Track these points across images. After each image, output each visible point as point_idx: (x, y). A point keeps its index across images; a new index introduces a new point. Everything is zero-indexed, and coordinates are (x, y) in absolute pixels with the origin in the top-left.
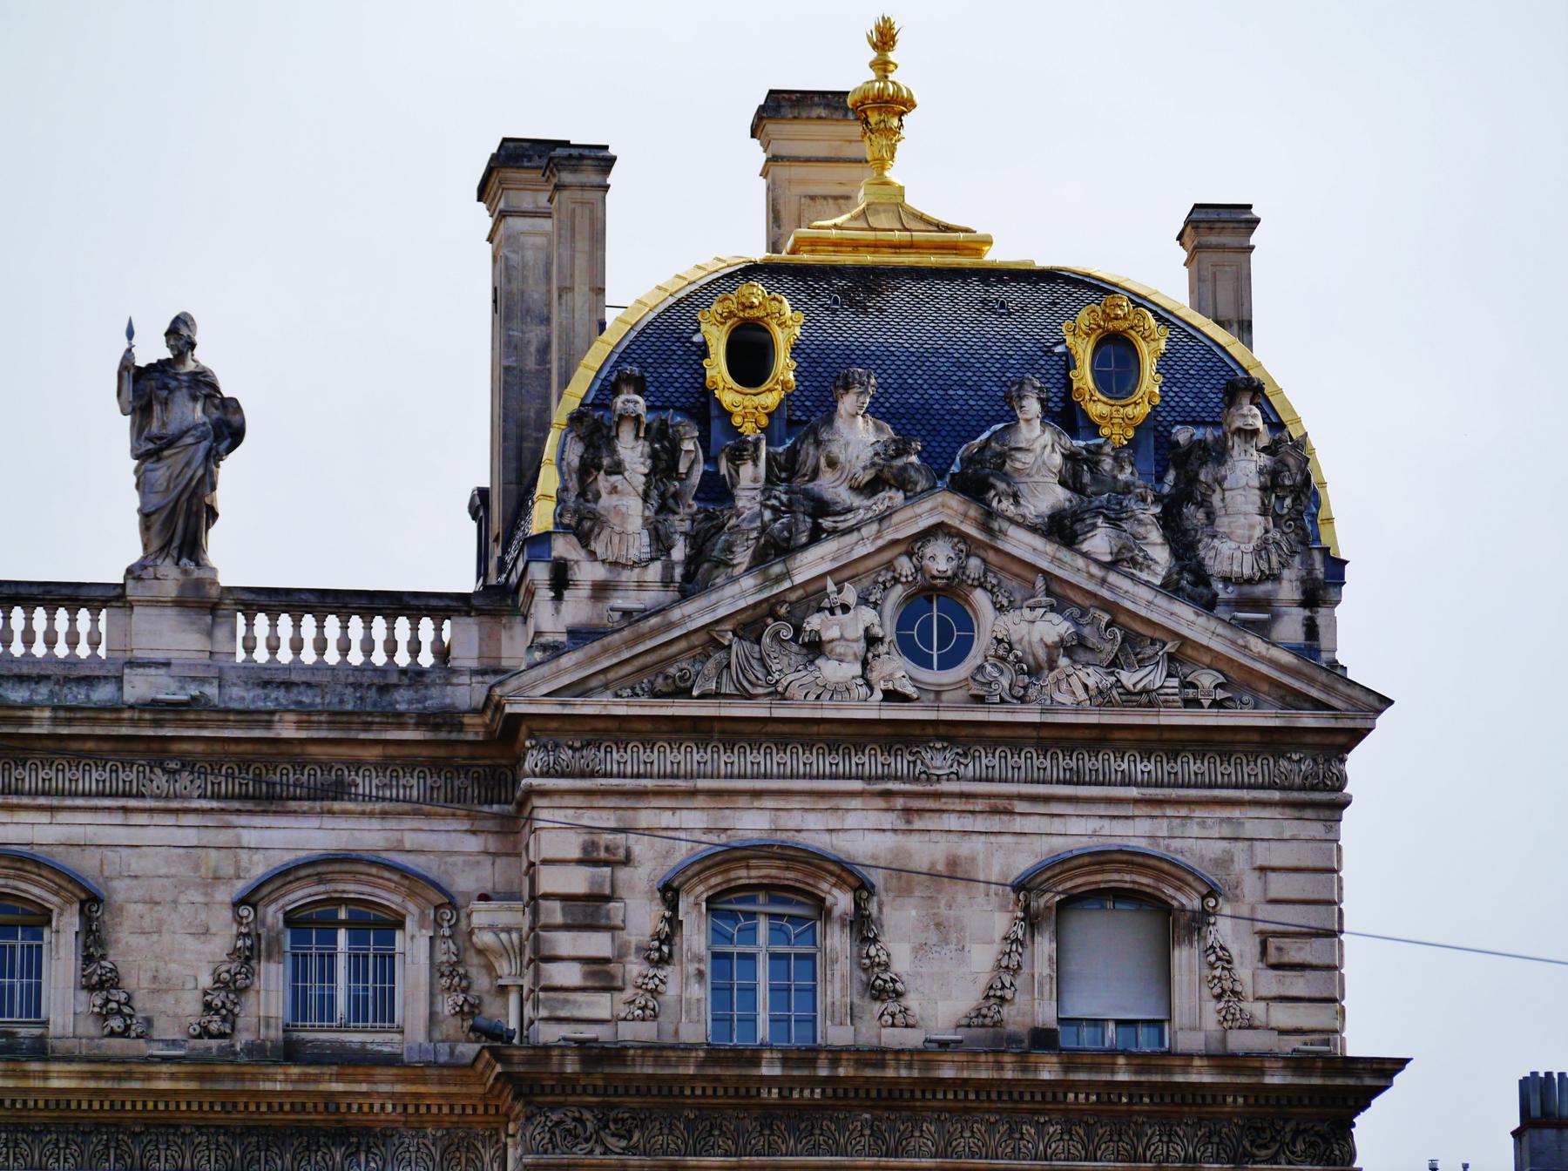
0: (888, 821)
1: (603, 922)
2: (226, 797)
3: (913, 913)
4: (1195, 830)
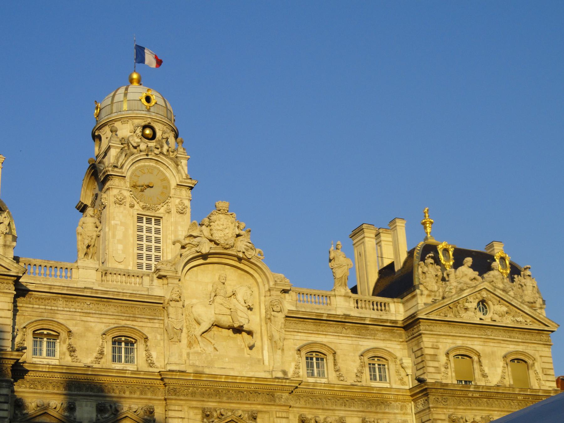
0: (481, 343)
1: (437, 360)
2: (356, 335)
3: (487, 361)
4: (529, 348)
